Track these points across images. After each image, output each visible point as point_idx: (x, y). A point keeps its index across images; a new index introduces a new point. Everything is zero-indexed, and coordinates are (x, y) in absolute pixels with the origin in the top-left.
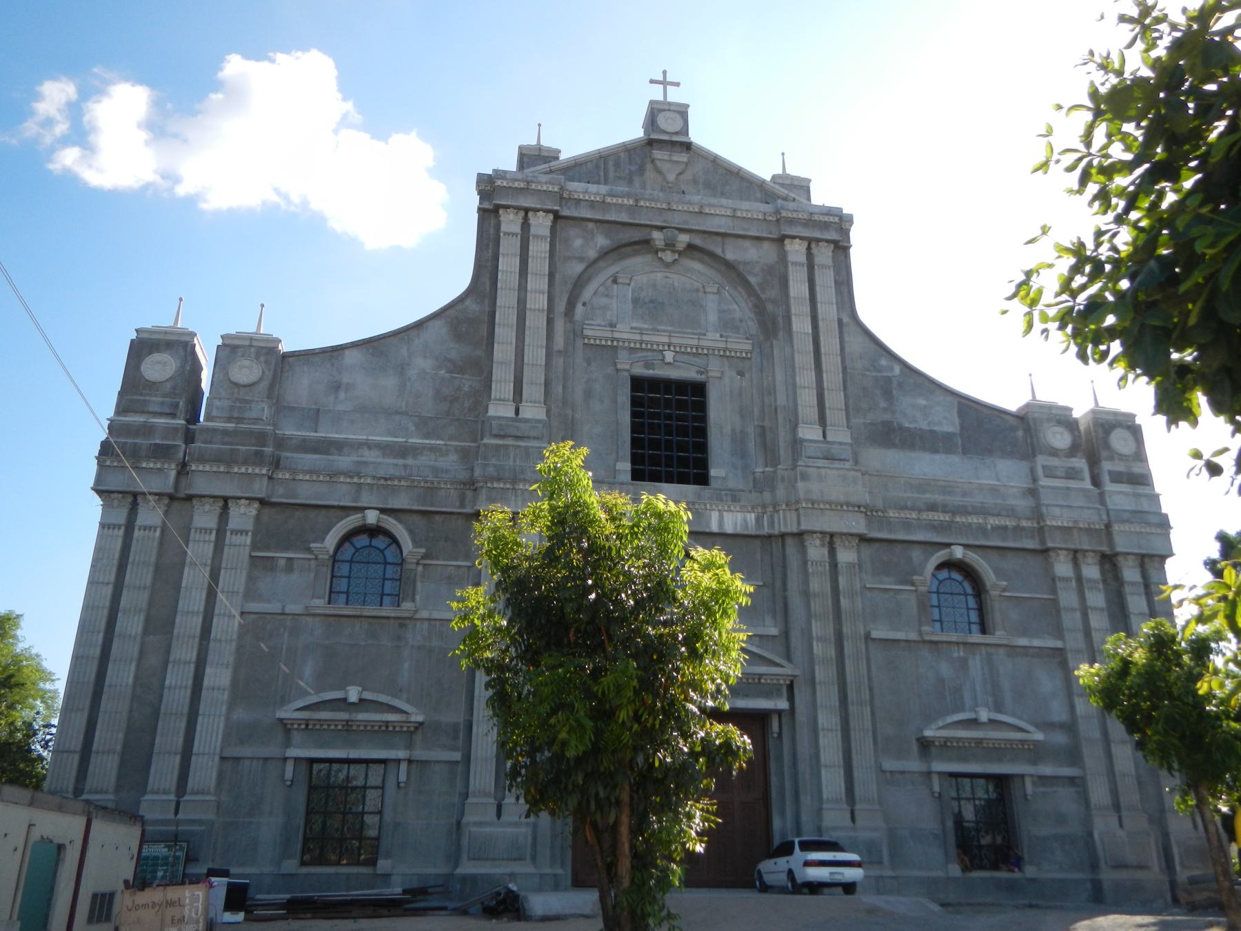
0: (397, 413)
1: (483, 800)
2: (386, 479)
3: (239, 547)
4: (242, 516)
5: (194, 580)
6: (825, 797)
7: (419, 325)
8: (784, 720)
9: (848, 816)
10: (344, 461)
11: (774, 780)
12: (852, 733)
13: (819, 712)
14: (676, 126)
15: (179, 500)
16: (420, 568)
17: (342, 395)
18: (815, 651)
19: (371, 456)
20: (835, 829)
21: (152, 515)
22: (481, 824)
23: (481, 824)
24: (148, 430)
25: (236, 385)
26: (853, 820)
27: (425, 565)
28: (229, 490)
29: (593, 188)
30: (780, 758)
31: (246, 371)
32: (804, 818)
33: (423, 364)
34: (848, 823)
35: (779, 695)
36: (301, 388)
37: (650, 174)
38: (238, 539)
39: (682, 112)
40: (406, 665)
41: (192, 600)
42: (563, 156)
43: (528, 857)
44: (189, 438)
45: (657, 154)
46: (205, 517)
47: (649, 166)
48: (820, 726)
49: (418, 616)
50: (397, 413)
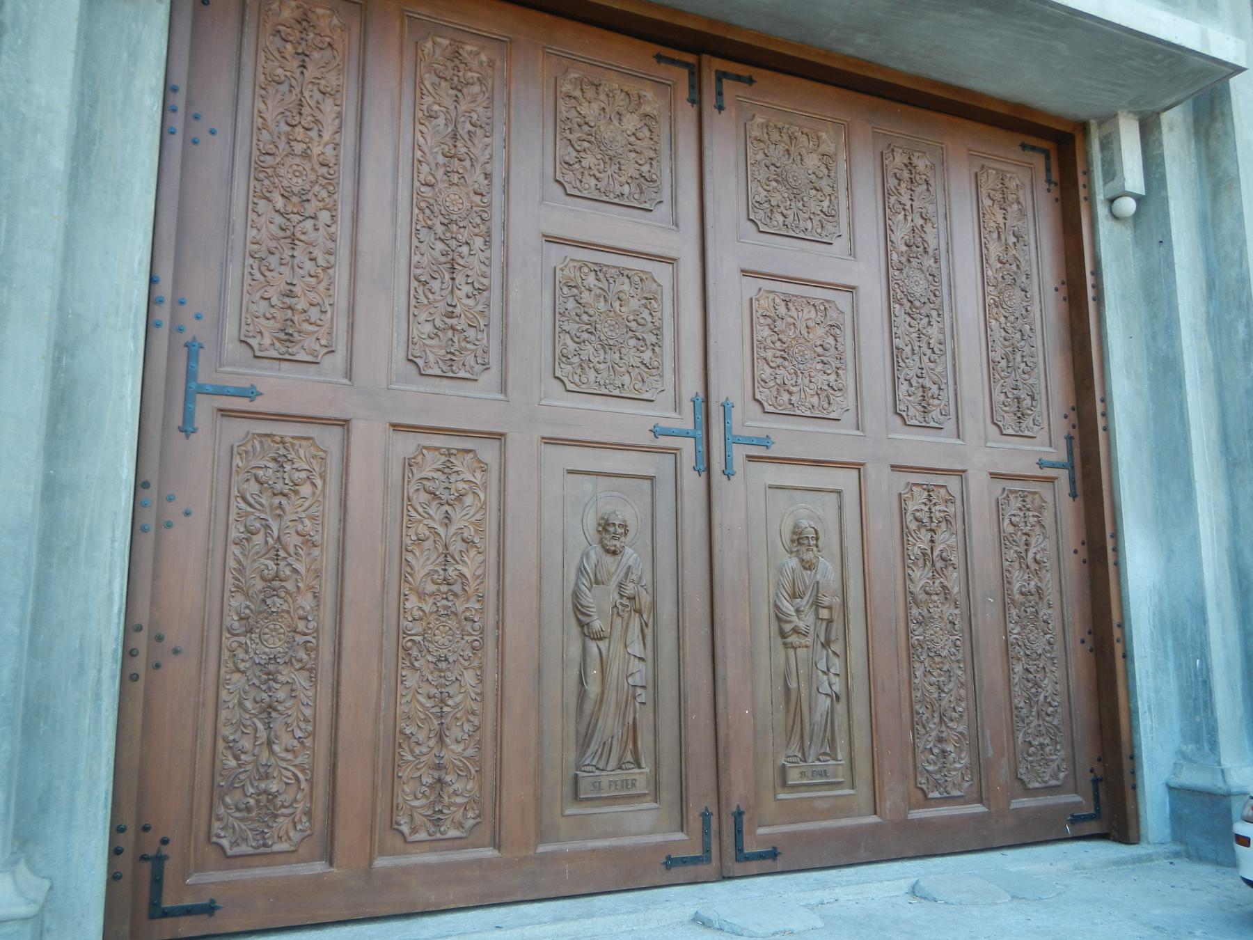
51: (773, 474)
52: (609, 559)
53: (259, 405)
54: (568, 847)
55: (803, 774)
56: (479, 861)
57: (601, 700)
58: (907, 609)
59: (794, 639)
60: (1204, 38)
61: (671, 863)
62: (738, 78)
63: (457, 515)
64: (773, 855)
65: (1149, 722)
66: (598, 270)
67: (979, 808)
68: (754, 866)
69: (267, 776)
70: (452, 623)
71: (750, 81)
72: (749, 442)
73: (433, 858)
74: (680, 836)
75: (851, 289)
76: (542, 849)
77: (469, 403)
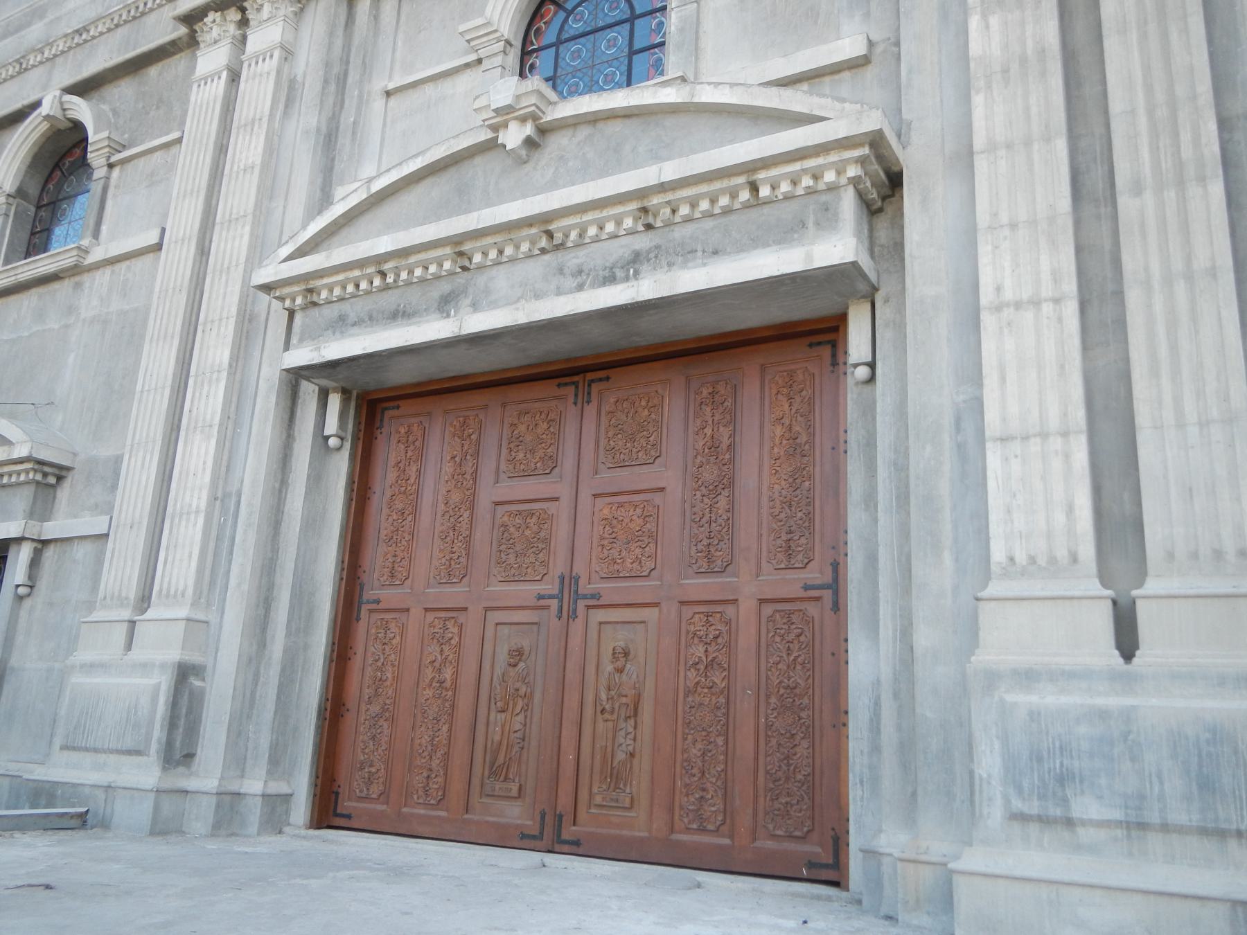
1: (114, 615)
2: (79, 32)
6: (998, 554)
8: (882, 311)
9: (1101, 622)
11: (855, 518)
12: (1134, 298)
13: (984, 250)
16: (116, 172)
18: (975, 47)
20: (1027, 677)
22: (89, 668)
23: (89, 668)
26: (1127, 639)
27: (123, 162)
30: (870, 443)
32: (924, 638)
34: (1116, 659)
35: (827, 219)
40: (72, 356)
43: (154, 747)
48: (986, 296)
49: (90, 259)
51: (599, 615)
52: (511, 669)
53: (381, 606)
54: (476, 818)
55: (604, 799)
56: (439, 817)
57: (500, 743)
58: (686, 696)
59: (607, 716)
60: (809, 257)
61: (524, 836)
62: (600, 380)
63: (446, 648)
64: (577, 843)
65: (859, 793)
66: (520, 513)
67: (727, 841)
68: (566, 848)
69: (371, 766)
70: (439, 702)
71: (608, 378)
72: (585, 597)
73: (422, 812)
74: (530, 823)
75: (662, 489)
76: (466, 816)
77: (454, 594)
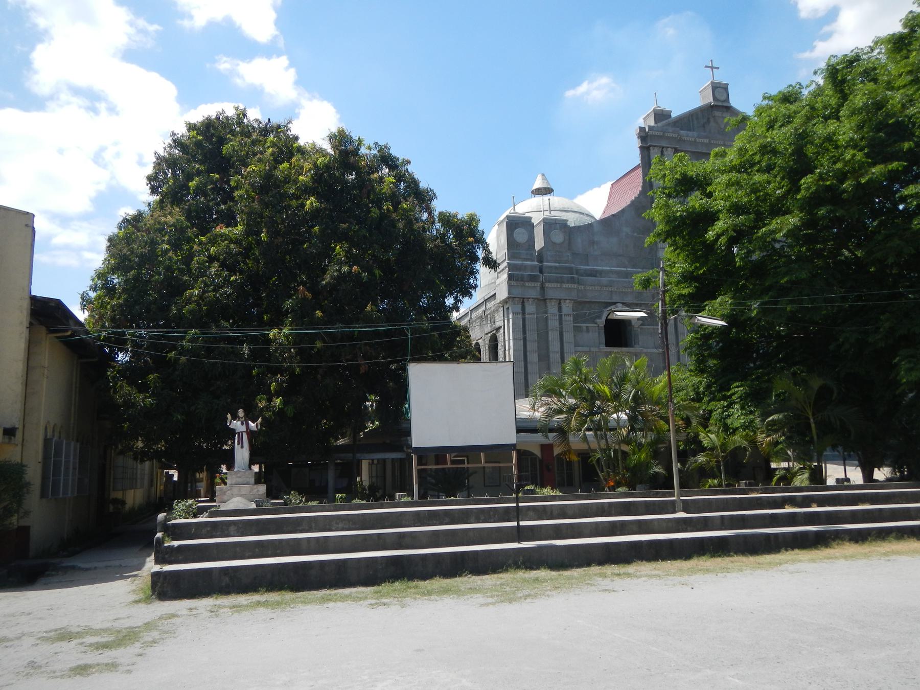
0: (620, 256)
3: (569, 320)
4: (567, 308)
5: (553, 337)
7: (623, 211)
10: (604, 280)
14: (723, 98)
15: (543, 300)
17: (595, 247)
19: (614, 278)
21: (530, 308)
24: (524, 268)
25: (555, 243)
28: (562, 295)
29: (690, 133)
31: (558, 237)
33: (626, 230)
36: (579, 243)
37: (712, 124)
38: (568, 318)
39: (725, 88)
41: (555, 346)
42: (673, 115)
44: (541, 271)
45: (717, 113)
46: (552, 309)
47: (712, 120)
50: (620, 256)
